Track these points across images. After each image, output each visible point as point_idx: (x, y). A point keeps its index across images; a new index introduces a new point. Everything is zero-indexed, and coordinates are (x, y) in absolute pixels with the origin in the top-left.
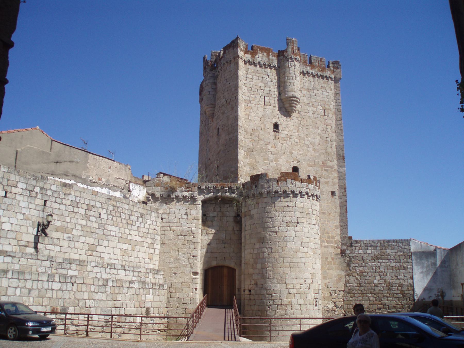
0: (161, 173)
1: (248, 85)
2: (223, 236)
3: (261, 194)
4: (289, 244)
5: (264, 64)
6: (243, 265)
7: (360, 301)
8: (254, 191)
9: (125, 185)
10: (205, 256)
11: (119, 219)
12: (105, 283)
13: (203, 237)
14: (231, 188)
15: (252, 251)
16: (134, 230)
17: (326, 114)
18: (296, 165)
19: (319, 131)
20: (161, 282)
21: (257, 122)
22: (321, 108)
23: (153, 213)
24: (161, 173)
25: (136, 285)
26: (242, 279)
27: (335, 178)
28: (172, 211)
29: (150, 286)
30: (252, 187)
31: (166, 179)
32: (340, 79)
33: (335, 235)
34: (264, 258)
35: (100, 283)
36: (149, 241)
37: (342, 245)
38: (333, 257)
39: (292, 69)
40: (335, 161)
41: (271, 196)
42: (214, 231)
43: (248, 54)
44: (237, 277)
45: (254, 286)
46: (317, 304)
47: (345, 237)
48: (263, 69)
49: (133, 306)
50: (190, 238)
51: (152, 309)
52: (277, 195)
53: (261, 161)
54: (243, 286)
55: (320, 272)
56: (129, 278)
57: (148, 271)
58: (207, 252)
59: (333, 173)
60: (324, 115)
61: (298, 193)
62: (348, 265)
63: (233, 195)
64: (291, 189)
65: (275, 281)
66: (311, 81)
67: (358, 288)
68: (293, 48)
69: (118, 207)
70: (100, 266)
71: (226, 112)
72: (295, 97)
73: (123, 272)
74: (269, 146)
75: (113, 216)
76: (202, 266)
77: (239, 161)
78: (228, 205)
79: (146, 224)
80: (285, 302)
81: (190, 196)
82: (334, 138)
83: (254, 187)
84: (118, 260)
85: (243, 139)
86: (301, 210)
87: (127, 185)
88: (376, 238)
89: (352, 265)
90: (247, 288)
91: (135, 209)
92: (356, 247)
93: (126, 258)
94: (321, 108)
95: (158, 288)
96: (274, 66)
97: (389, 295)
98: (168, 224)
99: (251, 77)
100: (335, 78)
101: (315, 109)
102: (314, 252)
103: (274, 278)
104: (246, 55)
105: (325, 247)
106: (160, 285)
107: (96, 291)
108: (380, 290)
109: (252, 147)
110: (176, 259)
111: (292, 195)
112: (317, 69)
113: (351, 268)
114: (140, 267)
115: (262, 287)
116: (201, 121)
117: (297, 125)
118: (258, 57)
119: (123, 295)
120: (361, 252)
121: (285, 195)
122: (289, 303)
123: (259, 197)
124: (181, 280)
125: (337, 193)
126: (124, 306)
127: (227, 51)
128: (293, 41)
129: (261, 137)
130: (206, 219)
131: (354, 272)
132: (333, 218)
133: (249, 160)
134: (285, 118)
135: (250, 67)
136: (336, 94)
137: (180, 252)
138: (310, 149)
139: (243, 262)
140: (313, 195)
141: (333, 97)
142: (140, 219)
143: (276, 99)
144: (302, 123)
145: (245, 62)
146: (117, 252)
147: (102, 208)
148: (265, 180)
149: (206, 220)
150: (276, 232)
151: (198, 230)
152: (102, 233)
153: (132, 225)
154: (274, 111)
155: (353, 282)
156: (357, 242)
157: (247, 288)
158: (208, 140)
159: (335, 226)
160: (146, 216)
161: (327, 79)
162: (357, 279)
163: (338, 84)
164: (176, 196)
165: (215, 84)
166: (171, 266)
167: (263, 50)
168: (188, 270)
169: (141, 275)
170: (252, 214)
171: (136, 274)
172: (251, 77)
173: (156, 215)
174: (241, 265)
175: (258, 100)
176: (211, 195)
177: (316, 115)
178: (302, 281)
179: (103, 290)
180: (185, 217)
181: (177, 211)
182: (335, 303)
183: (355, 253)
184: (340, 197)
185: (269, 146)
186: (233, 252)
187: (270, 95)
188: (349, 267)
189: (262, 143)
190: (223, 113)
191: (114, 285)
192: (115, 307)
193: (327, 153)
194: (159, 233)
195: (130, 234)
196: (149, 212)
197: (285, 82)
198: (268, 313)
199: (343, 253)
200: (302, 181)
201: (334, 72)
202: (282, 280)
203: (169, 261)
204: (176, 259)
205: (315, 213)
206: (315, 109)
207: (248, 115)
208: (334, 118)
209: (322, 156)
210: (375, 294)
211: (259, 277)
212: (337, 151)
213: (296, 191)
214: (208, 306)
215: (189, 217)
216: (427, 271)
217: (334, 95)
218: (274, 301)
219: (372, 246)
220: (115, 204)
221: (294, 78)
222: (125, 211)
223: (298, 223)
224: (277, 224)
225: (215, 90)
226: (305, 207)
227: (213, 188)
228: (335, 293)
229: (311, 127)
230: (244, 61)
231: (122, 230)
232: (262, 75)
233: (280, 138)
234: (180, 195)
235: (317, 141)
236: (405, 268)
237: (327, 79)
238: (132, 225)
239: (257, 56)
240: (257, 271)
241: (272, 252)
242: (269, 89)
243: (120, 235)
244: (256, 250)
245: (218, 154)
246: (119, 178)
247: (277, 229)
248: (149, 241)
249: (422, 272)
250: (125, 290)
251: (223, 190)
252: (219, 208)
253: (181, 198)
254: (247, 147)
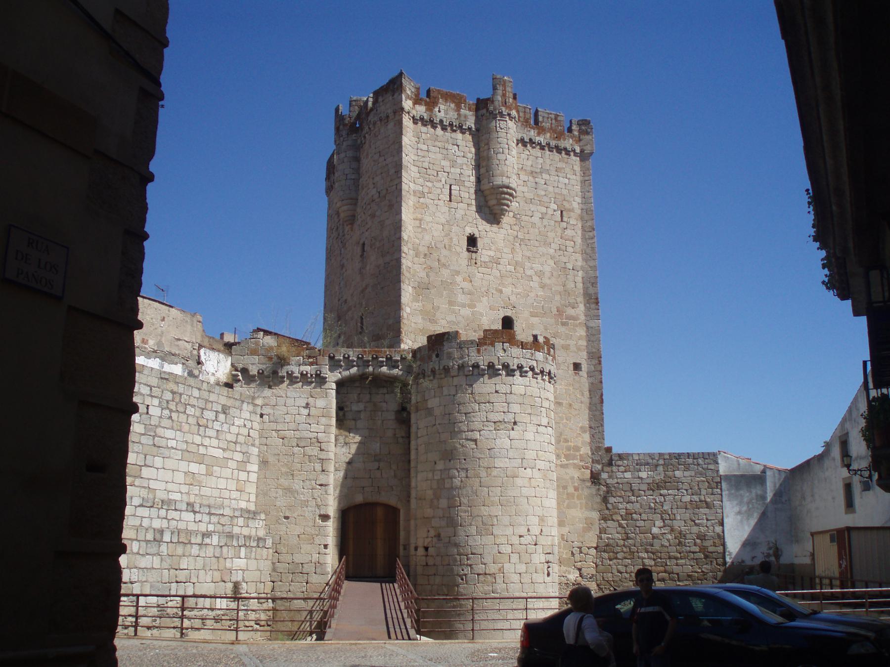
0: (259, 330)
1: (420, 164)
2: (376, 447)
3: (447, 370)
4: (499, 463)
5: (451, 125)
6: (413, 501)
7: (626, 566)
8: (434, 364)
9: (191, 352)
10: (343, 485)
11: (183, 417)
12: (158, 536)
13: (338, 450)
14: (391, 357)
15: (430, 475)
16: (210, 437)
17: (565, 219)
18: (509, 313)
19: (552, 251)
20: (261, 533)
21: (436, 234)
22: (555, 207)
23: (245, 405)
24: (259, 330)
25: (215, 540)
26: (412, 527)
27: (580, 338)
28: (281, 401)
29: (242, 542)
30: (430, 358)
31: (269, 341)
32: (591, 154)
33: (580, 445)
34: (452, 488)
35: (150, 537)
36: (238, 457)
37: (593, 462)
39: (502, 134)
40: (582, 307)
41: (466, 373)
42: (358, 438)
43: (420, 104)
44: (402, 523)
45: (435, 539)
46: (551, 572)
47: (598, 449)
48: (448, 134)
49: (209, 579)
50: (313, 451)
51: (244, 584)
52: (476, 372)
53: (444, 306)
54: (412, 541)
55: (555, 513)
56: (203, 528)
57: (237, 514)
58: (345, 477)
59: (577, 329)
60: (562, 221)
61: (515, 367)
62: (605, 500)
63: (395, 371)
64: (502, 362)
65: (473, 530)
66: (537, 157)
67: (622, 542)
68: (504, 95)
69: (181, 395)
70: (149, 505)
71: (378, 213)
72: (508, 187)
73: (190, 516)
74: (459, 279)
75: (171, 411)
76: (336, 504)
77: (403, 306)
78: (385, 391)
79: (233, 425)
80: (492, 568)
81: (313, 372)
82: (580, 263)
83: (434, 356)
84: (182, 493)
85: (410, 264)
86: (520, 400)
87: (195, 352)
88: (656, 449)
89: (612, 500)
90: (420, 543)
91: (213, 397)
92: (619, 466)
93: (196, 490)
94: (555, 207)
95: (255, 544)
96: (470, 129)
97: (679, 555)
98: (273, 426)
99: (425, 147)
100: (582, 151)
101: (544, 210)
102: (545, 478)
103: (471, 525)
104: (417, 107)
105: (562, 466)
106: (259, 539)
107: (141, 552)
108: (662, 546)
109: (426, 280)
110: (289, 490)
111: (504, 373)
112: (548, 135)
113: (609, 506)
114: (222, 506)
115: (449, 542)
116: (330, 230)
117: (511, 238)
118: (439, 111)
119: (191, 558)
120: (628, 475)
121: (491, 371)
122: (500, 570)
123: (443, 376)
124: (298, 530)
125: (584, 367)
126: (194, 580)
127: (380, 99)
128: (505, 81)
129: (443, 260)
130: (344, 415)
131: (616, 513)
132: (577, 412)
133: (420, 304)
134: (487, 226)
135: (424, 129)
136: (583, 182)
137: (295, 478)
138: (535, 285)
139: (413, 494)
140: (542, 372)
141: (578, 188)
142: (222, 417)
143: (472, 191)
144: (520, 235)
145: (415, 121)
146: (180, 477)
147: (152, 396)
148: (454, 344)
149: (343, 419)
150: (475, 441)
151: (329, 437)
152: (151, 443)
153: (207, 427)
154: (468, 212)
155: (614, 531)
156: (621, 457)
157: (420, 543)
158: (342, 266)
159: (581, 428)
160: (232, 411)
161: (568, 153)
162: (620, 525)
163: (587, 162)
164: (287, 372)
165: (357, 159)
166: (278, 504)
167: (449, 97)
168: (310, 512)
169: (223, 520)
170: (429, 406)
171: (214, 519)
172: (425, 147)
173: (251, 408)
174: (409, 501)
175: (439, 191)
176: (354, 370)
177: (545, 222)
178: (523, 530)
179: (153, 550)
180: (306, 412)
181: (290, 402)
182: (580, 570)
183: (617, 478)
184: (590, 375)
185: (459, 279)
186: (395, 476)
187: (460, 182)
188: (606, 504)
189: (445, 272)
190: (373, 216)
191: (175, 540)
192: (177, 582)
193: (567, 293)
194: (257, 442)
195: (202, 445)
196: (238, 403)
197: (489, 158)
198: (461, 590)
199: (595, 478)
200: (523, 345)
201: (580, 140)
202: (486, 529)
203: (274, 495)
204: (289, 490)
205: (546, 404)
206: (544, 210)
207: (421, 220)
208: (580, 225)
209: (557, 298)
210: (653, 553)
211: (443, 523)
212: (585, 289)
213: (511, 364)
214: (349, 578)
215: (313, 411)
216: (749, 510)
217: (579, 184)
218: (472, 568)
219: (648, 464)
220: (175, 389)
221: (506, 151)
222: (193, 401)
223: (515, 423)
224: (477, 425)
225: (357, 171)
226: (528, 393)
227: (358, 358)
228: (581, 552)
229: (537, 244)
230: (413, 117)
231: (189, 438)
232: (446, 145)
233: (479, 264)
234: (296, 371)
235: (547, 269)
236: (708, 506)
237: (566, 154)
238: (207, 427)
239: (437, 109)
240: (440, 513)
241: (467, 477)
242: (458, 171)
243: (184, 446)
244: (439, 473)
245: (363, 291)
246: (179, 340)
247: (477, 435)
248: (238, 457)
249: (739, 513)
250: (195, 550)
251: (375, 362)
252: (368, 396)
253: (297, 377)
254: (418, 280)
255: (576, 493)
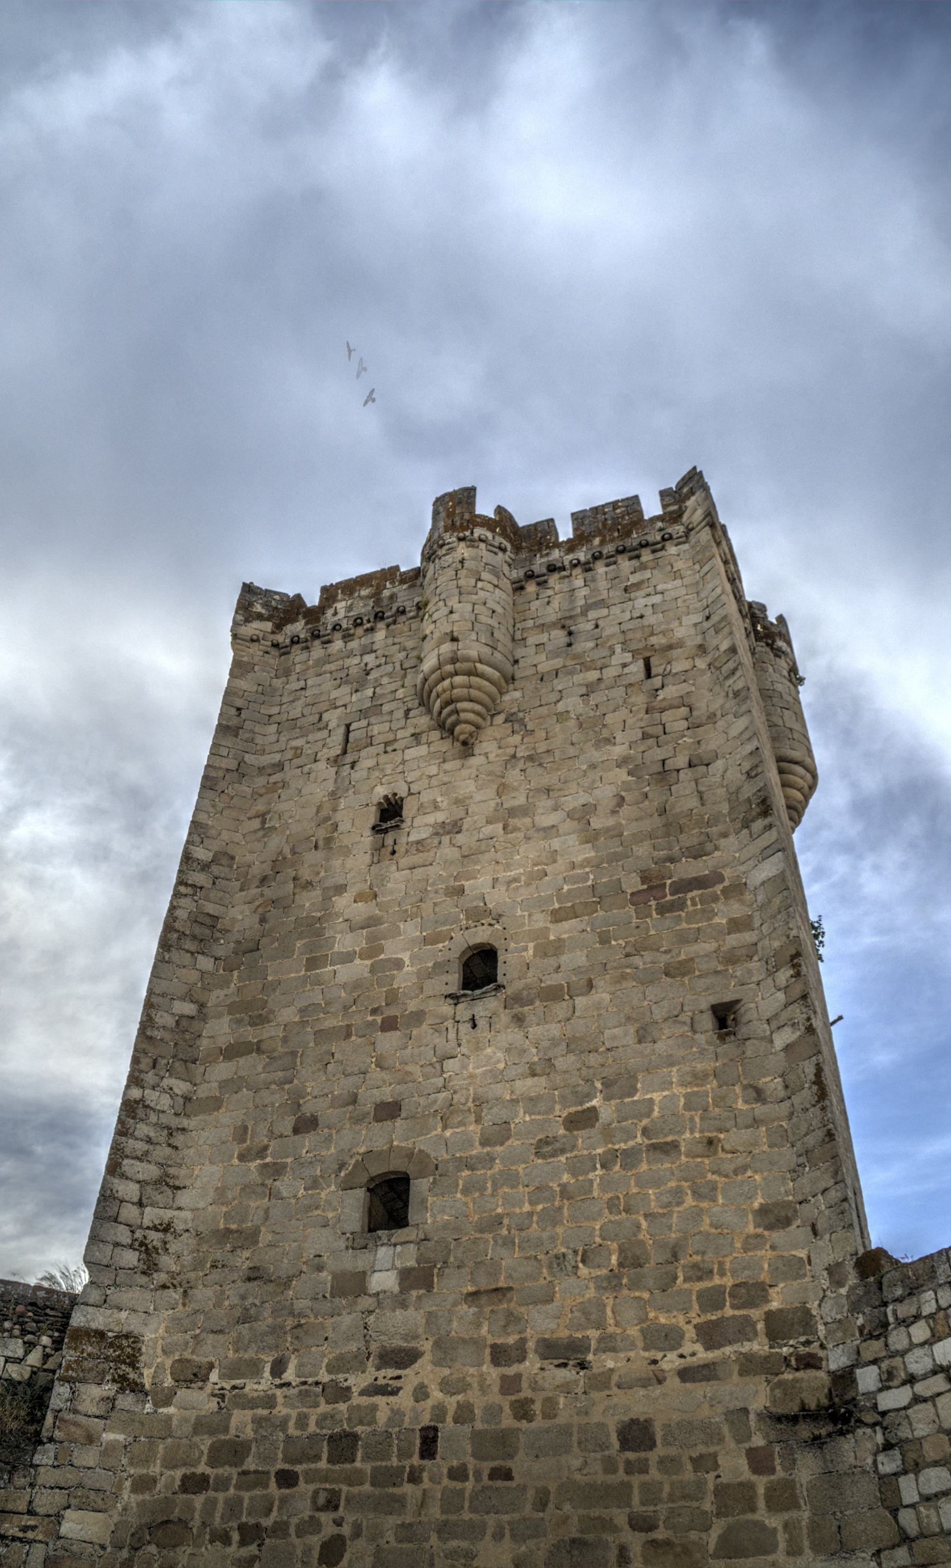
18: (481, 935)
33: (764, 1277)
38: (758, 1441)
59: (719, 906)
118: (336, 614)
159: (763, 1211)
209: (642, 850)
235: (605, 793)
255: (761, 1483)
